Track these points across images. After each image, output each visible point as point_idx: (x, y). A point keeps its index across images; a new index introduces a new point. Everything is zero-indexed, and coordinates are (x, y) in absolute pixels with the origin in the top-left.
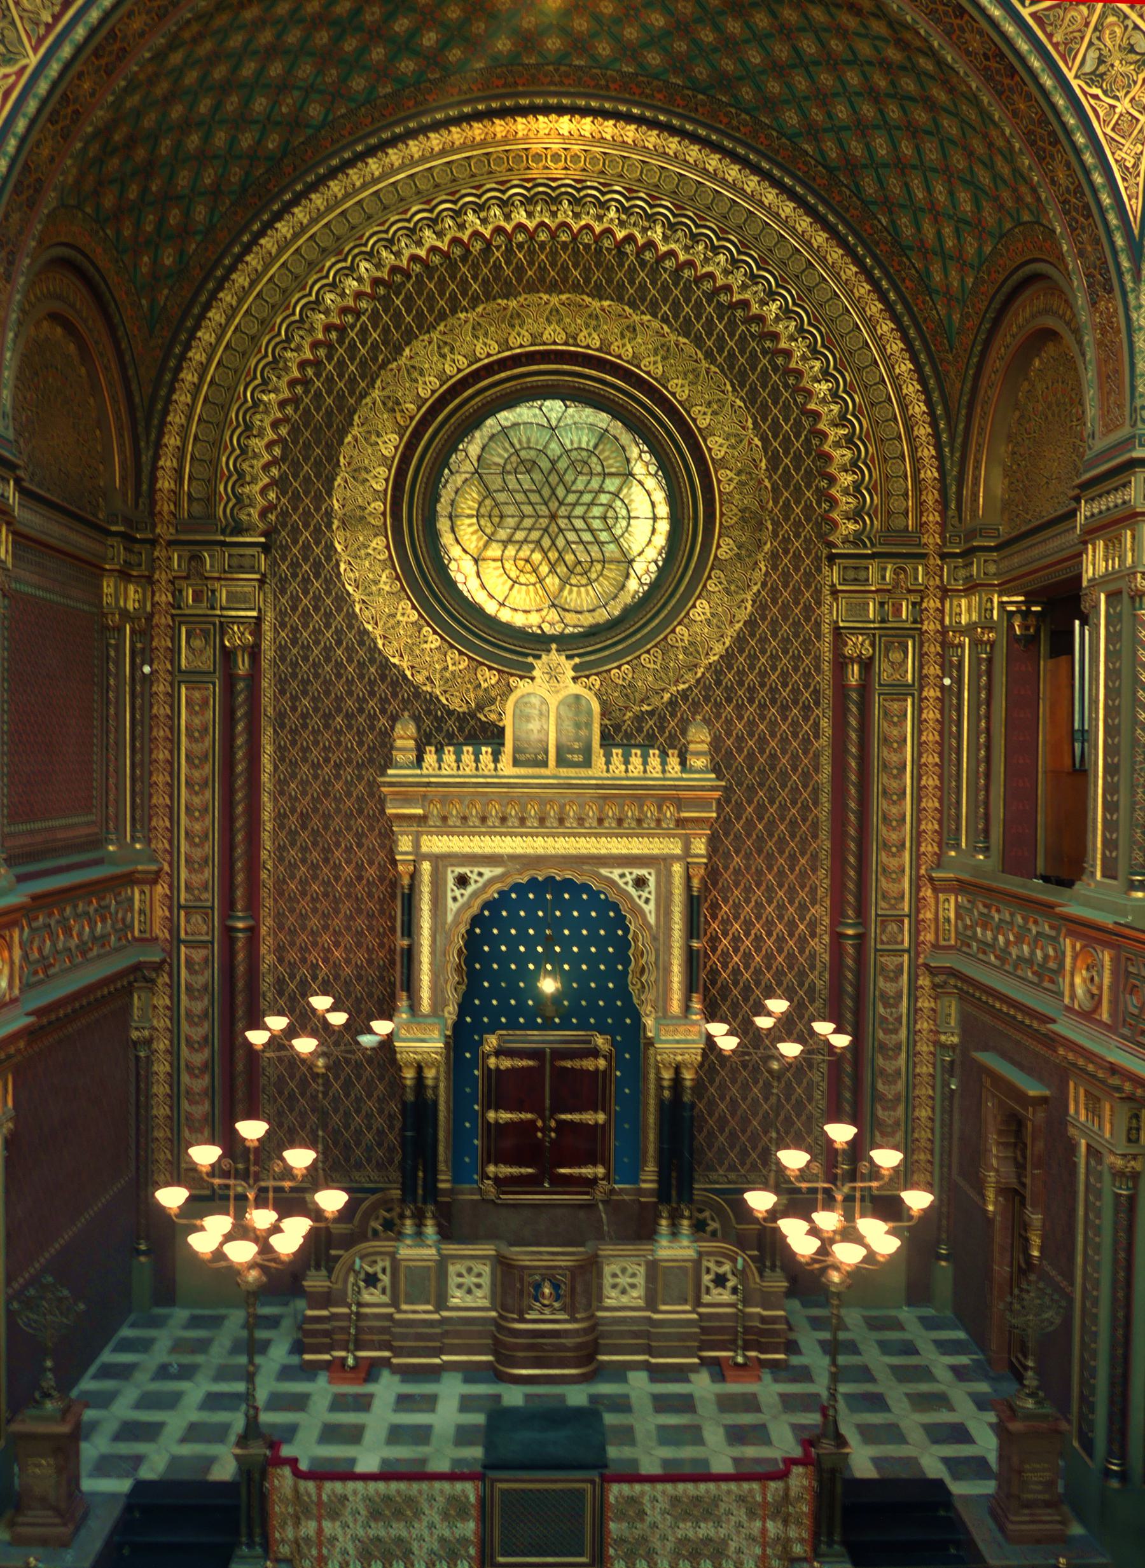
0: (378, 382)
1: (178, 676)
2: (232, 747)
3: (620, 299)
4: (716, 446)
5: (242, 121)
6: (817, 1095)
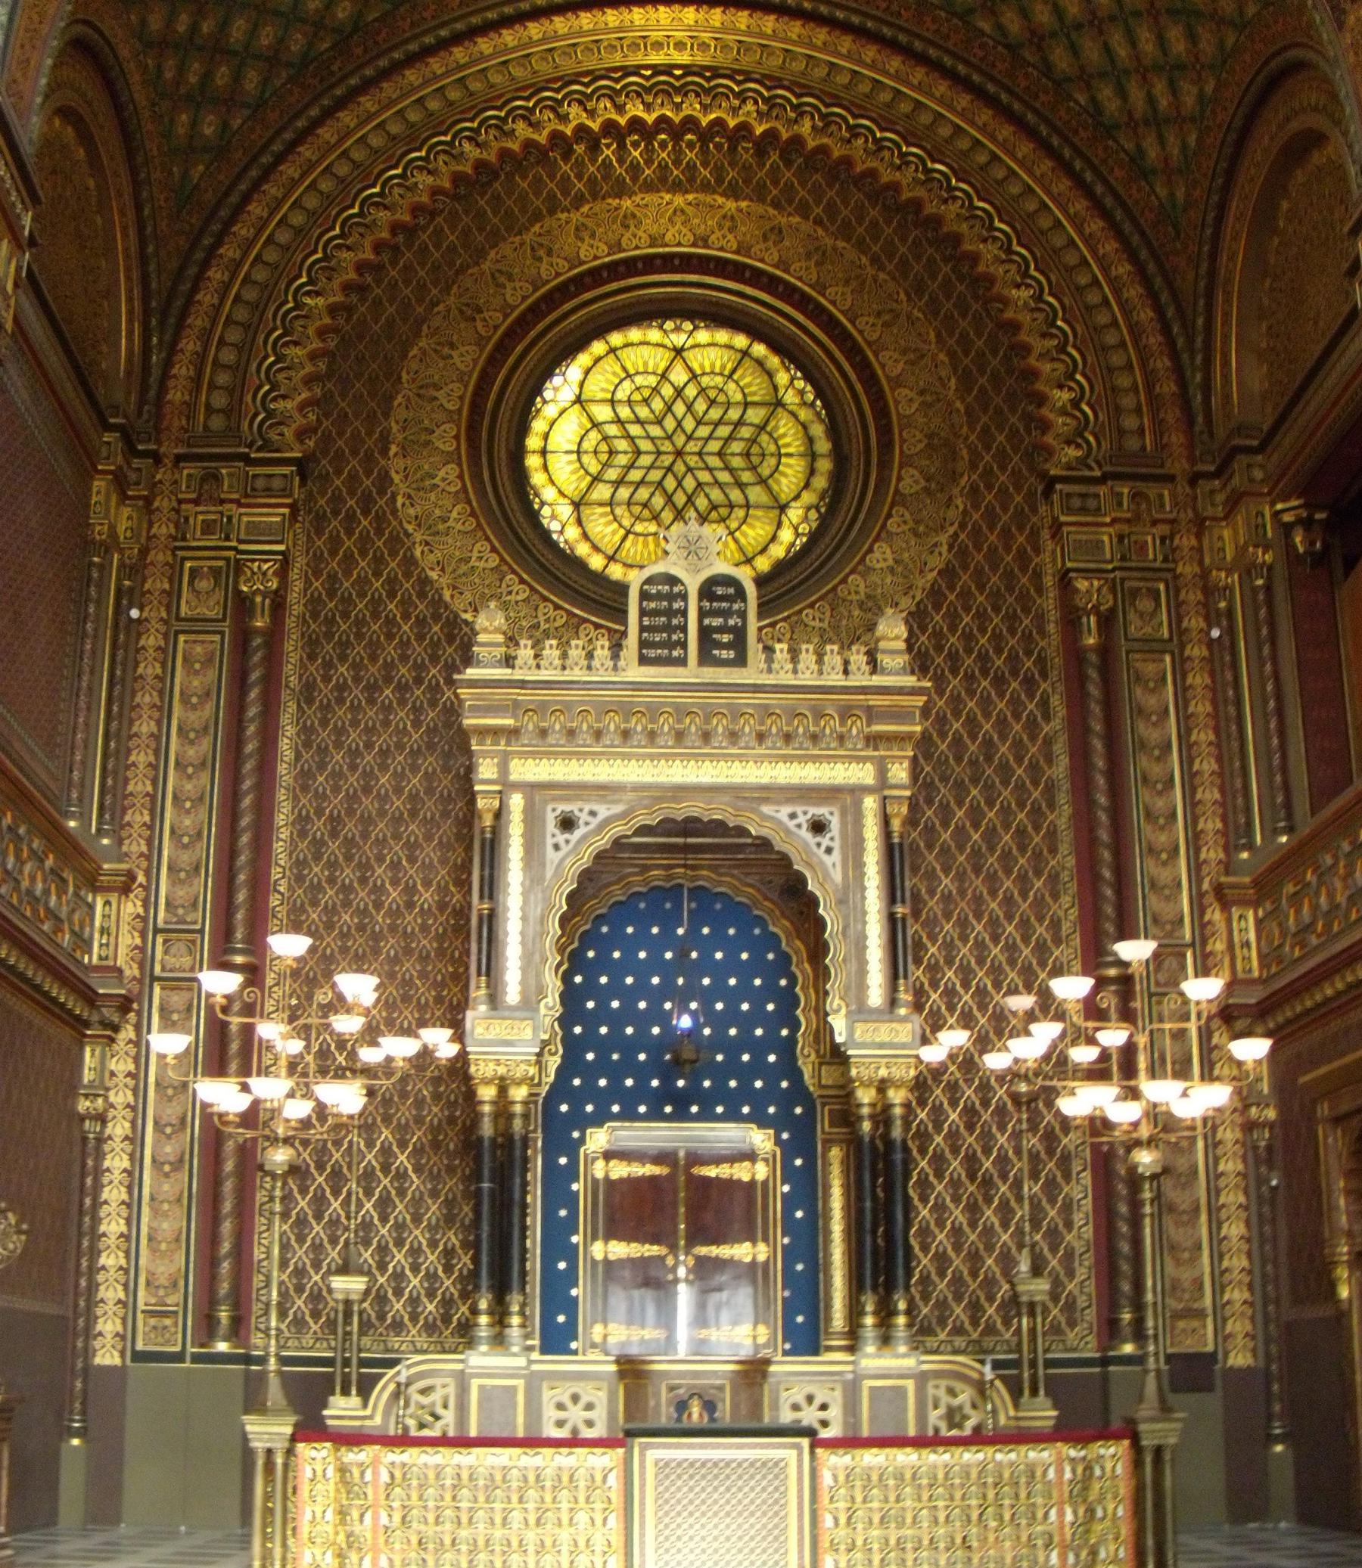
0: (455, 289)
1: (175, 625)
2: (240, 721)
3: (761, 199)
6: (1078, 1219)
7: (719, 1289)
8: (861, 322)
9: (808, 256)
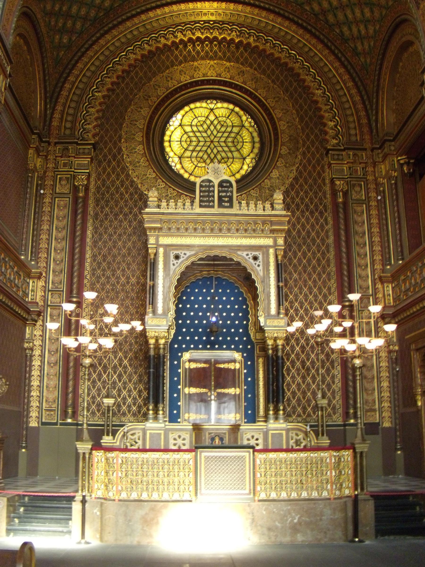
1: (55, 195)
2: (75, 225)
3: (238, 62)
6: (336, 381)
7: (224, 403)
8: (269, 101)
9: (252, 80)
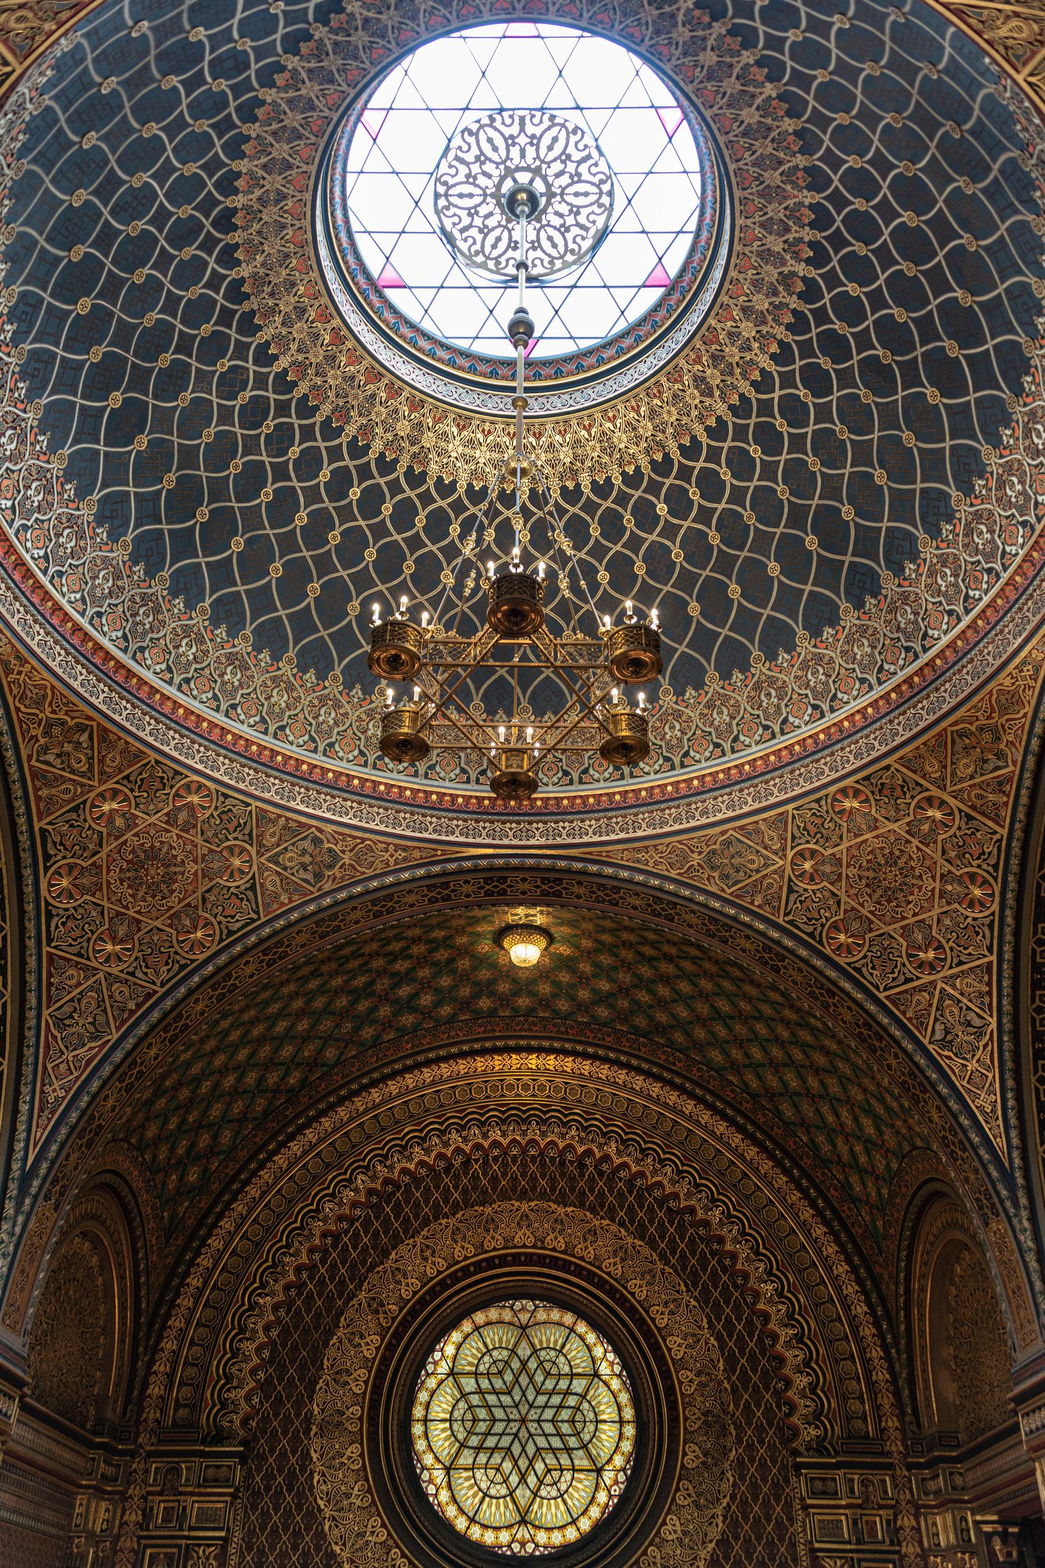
3: (582, 1206)
4: (676, 1346)
5: (270, 1064)
